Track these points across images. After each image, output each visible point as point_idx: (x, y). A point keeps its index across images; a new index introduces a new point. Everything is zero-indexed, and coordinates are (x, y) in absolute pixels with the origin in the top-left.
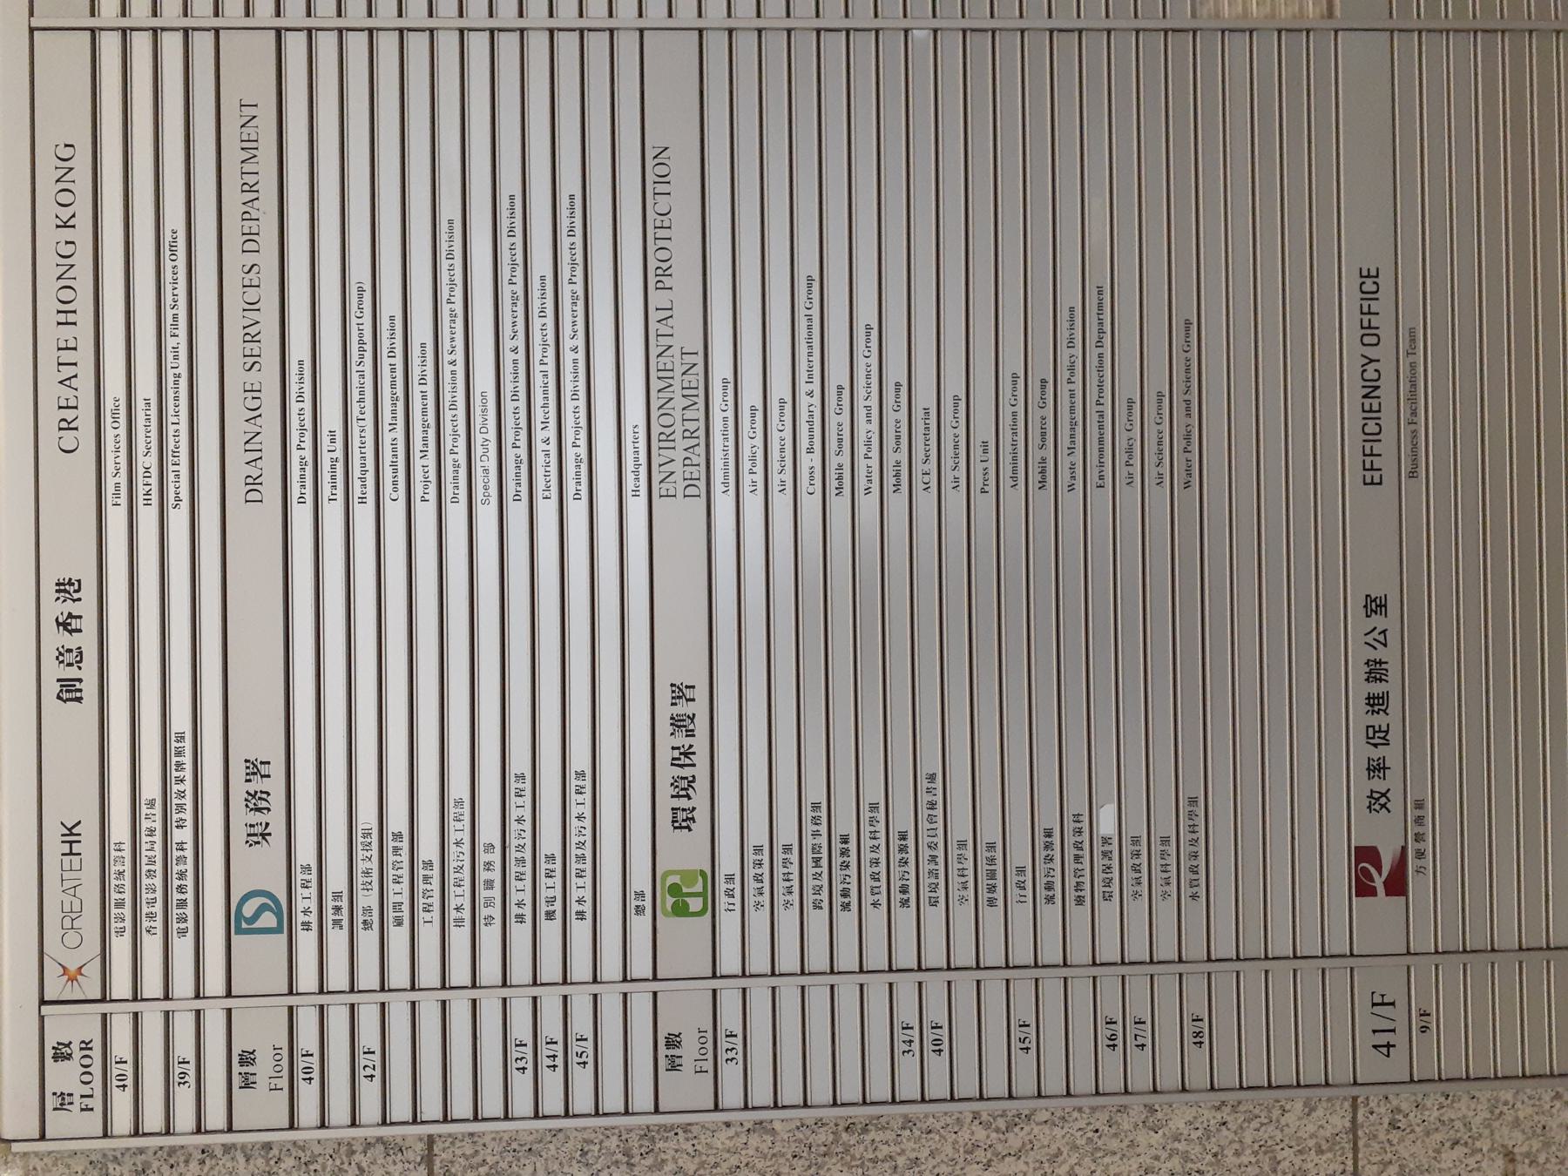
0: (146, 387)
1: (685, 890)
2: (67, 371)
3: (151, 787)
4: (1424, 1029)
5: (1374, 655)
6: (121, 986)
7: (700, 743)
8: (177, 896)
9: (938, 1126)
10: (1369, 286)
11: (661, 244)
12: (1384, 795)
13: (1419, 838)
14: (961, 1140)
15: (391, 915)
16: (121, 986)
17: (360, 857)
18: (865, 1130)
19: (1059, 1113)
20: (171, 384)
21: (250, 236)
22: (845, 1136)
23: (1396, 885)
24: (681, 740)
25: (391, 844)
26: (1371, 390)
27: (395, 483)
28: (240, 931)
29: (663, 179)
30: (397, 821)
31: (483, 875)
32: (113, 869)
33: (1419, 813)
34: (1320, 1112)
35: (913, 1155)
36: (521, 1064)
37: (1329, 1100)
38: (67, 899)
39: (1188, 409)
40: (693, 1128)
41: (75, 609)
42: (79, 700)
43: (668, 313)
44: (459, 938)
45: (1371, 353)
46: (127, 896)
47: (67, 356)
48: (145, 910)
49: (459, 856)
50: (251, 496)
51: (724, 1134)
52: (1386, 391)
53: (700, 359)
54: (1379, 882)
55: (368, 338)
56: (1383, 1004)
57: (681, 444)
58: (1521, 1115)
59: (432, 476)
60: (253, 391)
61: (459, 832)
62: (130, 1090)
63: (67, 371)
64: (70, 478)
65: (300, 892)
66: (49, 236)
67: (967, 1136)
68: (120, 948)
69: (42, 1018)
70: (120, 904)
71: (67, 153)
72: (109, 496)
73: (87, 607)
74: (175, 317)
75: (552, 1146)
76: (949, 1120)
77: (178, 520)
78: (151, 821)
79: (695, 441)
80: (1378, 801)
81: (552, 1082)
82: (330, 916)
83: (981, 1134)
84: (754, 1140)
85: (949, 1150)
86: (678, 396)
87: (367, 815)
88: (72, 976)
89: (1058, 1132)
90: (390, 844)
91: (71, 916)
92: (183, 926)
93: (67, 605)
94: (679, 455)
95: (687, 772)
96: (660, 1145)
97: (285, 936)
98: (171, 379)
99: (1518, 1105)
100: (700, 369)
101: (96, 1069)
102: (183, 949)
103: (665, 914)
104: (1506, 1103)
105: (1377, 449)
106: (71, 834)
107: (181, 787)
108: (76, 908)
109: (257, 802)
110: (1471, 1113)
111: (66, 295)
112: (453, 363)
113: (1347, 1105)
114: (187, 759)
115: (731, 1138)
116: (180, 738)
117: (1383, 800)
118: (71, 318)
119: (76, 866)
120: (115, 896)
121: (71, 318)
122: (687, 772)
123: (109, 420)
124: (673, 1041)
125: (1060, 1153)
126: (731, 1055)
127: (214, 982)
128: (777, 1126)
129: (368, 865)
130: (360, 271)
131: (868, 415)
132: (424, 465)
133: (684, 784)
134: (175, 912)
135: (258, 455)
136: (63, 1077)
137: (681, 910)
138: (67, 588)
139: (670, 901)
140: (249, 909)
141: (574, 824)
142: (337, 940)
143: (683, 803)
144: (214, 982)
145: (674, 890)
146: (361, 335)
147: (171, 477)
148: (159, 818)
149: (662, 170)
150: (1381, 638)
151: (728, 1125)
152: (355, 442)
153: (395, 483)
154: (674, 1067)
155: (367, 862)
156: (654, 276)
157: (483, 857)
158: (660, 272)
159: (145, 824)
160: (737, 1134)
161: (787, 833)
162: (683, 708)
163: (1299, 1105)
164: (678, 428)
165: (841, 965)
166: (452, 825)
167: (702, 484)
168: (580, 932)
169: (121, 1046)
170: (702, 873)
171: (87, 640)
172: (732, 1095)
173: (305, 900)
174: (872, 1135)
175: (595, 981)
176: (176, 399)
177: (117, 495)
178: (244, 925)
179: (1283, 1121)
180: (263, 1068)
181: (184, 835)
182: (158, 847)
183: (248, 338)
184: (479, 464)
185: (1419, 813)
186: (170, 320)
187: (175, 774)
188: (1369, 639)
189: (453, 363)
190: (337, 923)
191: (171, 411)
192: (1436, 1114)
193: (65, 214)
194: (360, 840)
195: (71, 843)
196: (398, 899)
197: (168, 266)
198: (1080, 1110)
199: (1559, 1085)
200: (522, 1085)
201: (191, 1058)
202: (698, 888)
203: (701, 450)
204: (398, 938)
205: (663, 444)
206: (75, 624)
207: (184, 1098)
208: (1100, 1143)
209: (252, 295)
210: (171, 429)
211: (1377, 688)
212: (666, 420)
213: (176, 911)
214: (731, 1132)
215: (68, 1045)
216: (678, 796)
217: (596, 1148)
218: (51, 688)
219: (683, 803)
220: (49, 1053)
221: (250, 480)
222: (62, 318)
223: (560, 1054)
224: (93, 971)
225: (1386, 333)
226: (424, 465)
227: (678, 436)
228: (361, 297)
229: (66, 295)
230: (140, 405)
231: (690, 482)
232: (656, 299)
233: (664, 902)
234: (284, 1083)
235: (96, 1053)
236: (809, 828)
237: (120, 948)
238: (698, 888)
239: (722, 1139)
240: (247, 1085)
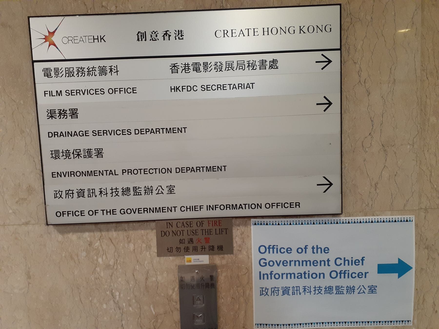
2: (246, 33)
38: (79, 38)
42: (138, 40)
47: (251, 32)
63: (246, 33)
71: (328, 29)
108: (76, 41)
111: (274, 31)
118: (266, 33)
121: (266, 33)
193: (305, 30)
222: (266, 30)
229: (274, 31)
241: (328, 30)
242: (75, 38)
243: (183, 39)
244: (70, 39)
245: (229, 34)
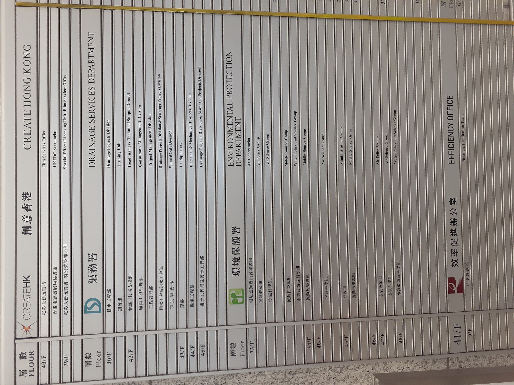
0: (55, 127)
1: (237, 295)
2: (27, 122)
3: (55, 263)
4: (470, 335)
5: (452, 217)
6: (44, 332)
7: (241, 247)
8: (64, 301)
9: (318, 371)
10: (450, 101)
11: (229, 83)
12: (456, 261)
13: (467, 274)
14: (325, 376)
15: (138, 306)
16: (44, 332)
17: (128, 285)
18: (295, 373)
19: (357, 366)
20: (63, 126)
21: (91, 78)
22: (288, 376)
23: (461, 290)
24: (235, 246)
25: (139, 282)
26: (451, 134)
27: (140, 161)
28: (86, 312)
29: (229, 62)
30: (141, 274)
31: (169, 292)
32: (42, 292)
33: (467, 267)
34: (437, 363)
35: (310, 381)
36: (182, 355)
37: (440, 359)
38: (25, 303)
39: (395, 138)
40: (239, 375)
41: (29, 203)
42: (30, 234)
43: (231, 106)
44: (162, 314)
45: (450, 122)
46: (47, 301)
47: (27, 117)
48: (53, 305)
49: (162, 286)
50: (91, 165)
51: (249, 376)
52: (455, 134)
53: (241, 121)
54: (455, 289)
55: (131, 112)
56: (457, 328)
57: (235, 149)
58: (498, 362)
59: (153, 158)
60: (92, 130)
61: (162, 278)
62: (47, 367)
63: (27, 122)
64: (27, 159)
65: (107, 299)
66: (21, 75)
67: (328, 374)
68: (44, 319)
69: (15, 344)
70: (44, 304)
72: (42, 164)
73: (33, 202)
74: (65, 104)
75: (192, 383)
76: (322, 369)
77: (66, 173)
78: (55, 274)
79: (240, 148)
80: (455, 263)
81: (193, 361)
82: (117, 306)
83: (332, 374)
84: (259, 378)
85: (321, 379)
86: (234, 133)
87: (130, 271)
88: (27, 329)
89: (356, 372)
90: (138, 282)
91: (27, 308)
92: (66, 311)
93: (26, 201)
94: (234, 152)
95: (237, 256)
96: (228, 381)
98: (63, 125)
99: (498, 359)
100: (241, 124)
101: (35, 361)
102: (66, 319)
103: (230, 303)
104: (494, 358)
105: (453, 152)
106: (27, 280)
107: (66, 263)
108: (28, 305)
109: (92, 268)
110: (483, 362)
111: (27, 96)
112: (160, 122)
113: (446, 360)
114: (68, 254)
115: (251, 378)
116: (66, 246)
117: (456, 263)
118: (29, 104)
119: (28, 291)
120: (42, 301)
121: (29, 104)
122: (237, 256)
123: (42, 138)
124: (233, 346)
125: (357, 379)
126: (252, 350)
127: (77, 330)
128: (266, 373)
129: (131, 288)
130: (129, 89)
131: (296, 140)
132: (150, 154)
133: (236, 260)
134: (63, 306)
135: (94, 151)
136: (23, 365)
137: (235, 302)
138: (26, 196)
139: (232, 299)
140: (89, 305)
141: (200, 274)
142: (120, 314)
143: (236, 266)
144: (77, 330)
145: (233, 295)
146: (129, 111)
147: (63, 158)
148: (58, 273)
149: (229, 60)
150: (455, 212)
151: (250, 373)
152: (127, 146)
153: (140, 161)
154: (233, 354)
155: (130, 287)
156: (227, 94)
157: (169, 286)
158: (228, 92)
159: (53, 276)
160: (253, 376)
162: (236, 235)
163: (431, 361)
164: (234, 143)
166: (159, 275)
167: (242, 162)
168: (202, 310)
169: (44, 352)
170: (242, 290)
171: (33, 213)
172: (252, 363)
173: (109, 301)
174: (297, 375)
176: (65, 132)
177: (44, 163)
178: (88, 310)
179: (426, 366)
180: (94, 359)
181: (67, 280)
182: (58, 283)
183: (90, 112)
184: (169, 154)
185: (467, 267)
186: (63, 105)
187: (64, 259)
188: (451, 212)
189: (160, 122)
190: (120, 309)
191: (63, 136)
192: (473, 362)
193: (27, 68)
194: (128, 280)
195: (27, 283)
196: (141, 300)
197: (63, 87)
198: (363, 365)
199: (510, 352)
200: (183, 362)
201: (69, 355)
202: (241, 295)
203: (242, 151)
204: (141, 314)
205: (229, 149)
206: (29, 208)
207: (66, 370)
208: (370, 375)
209: (92, 97)
210: (64, 142)
211: (454, 227)
212: (230, 141)
213: (64, 306)
214: (251, 376)
215: (25, 353)
216: (234, 264)
217: (206, 383)
218: (20, 230)
219: (236, 266)
220: (18, 356)
221: (91, 159)
222: (25, 104)
223: (196, 351)
224: (34, 327)
225: (455, 116)
226: (150, 154)
227: (234, 146)
228: (129, 98)
229: (27, 96)
230: (53, 133)
231: (238, 161)
232: (227, 101)
233: (230, 299)
234: (101, 364)
235: (35, 356)
237: (44, 319)
238: (241, 295)
239: (248, 378)
240: (88, 365)
241: (28, 48)
242: (25, 306)
243: (31, 193)
244: (25, 311)
245: (28, 136)
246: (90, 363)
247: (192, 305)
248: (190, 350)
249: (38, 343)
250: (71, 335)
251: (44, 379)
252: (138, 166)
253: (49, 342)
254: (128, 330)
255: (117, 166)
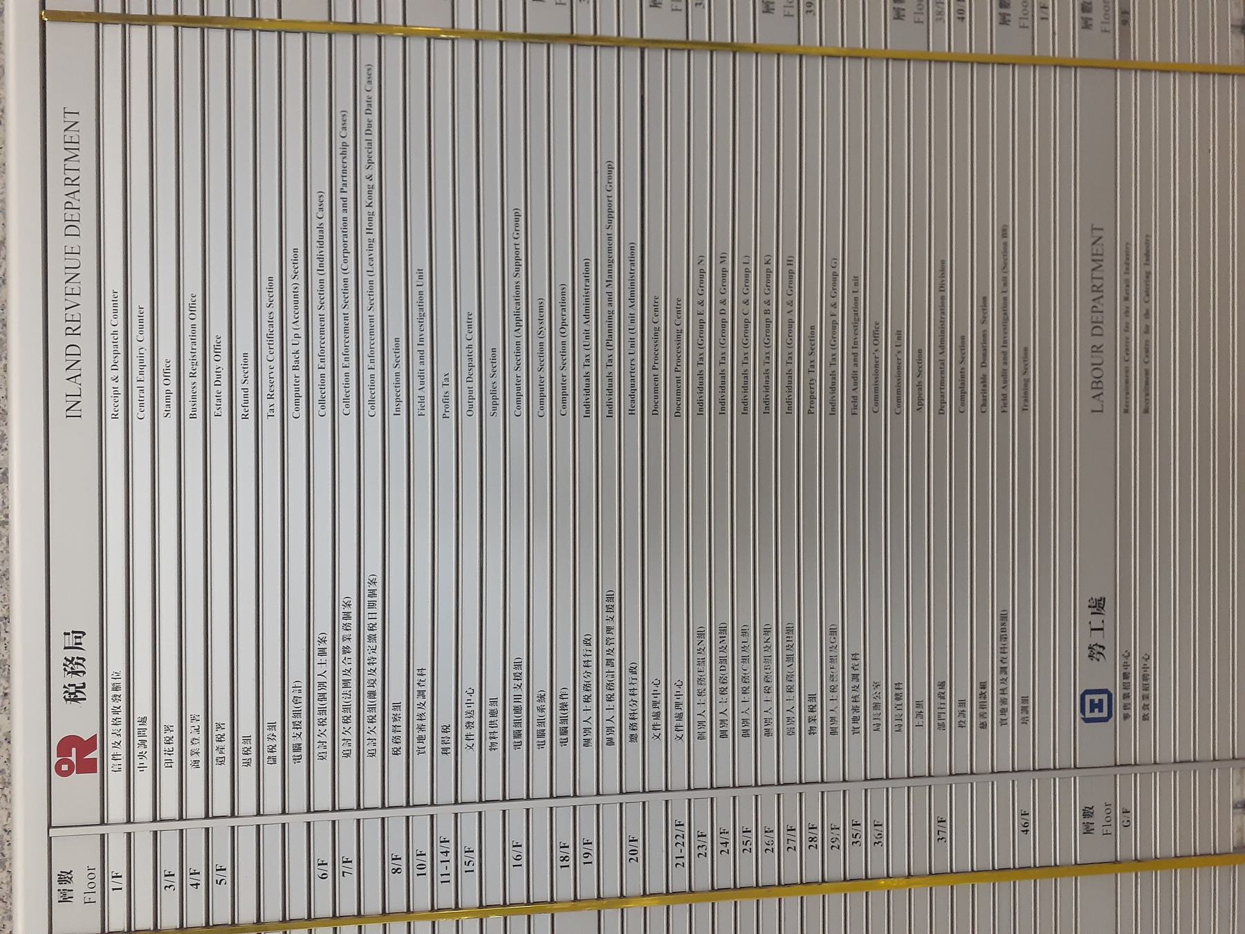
97: (98, 774)
161: (494, 689)
165: (488, 795)
175: (284, 812)
236: (511, 682)
246: (69, 894)
247: (587, 743)
248: (415, 861)
249: (103, 836)
250: (155, 820)
251: (117, 921)
252: (367, 416)
253: (155, 833)
254: (163, 817)
255: (265, 416)
